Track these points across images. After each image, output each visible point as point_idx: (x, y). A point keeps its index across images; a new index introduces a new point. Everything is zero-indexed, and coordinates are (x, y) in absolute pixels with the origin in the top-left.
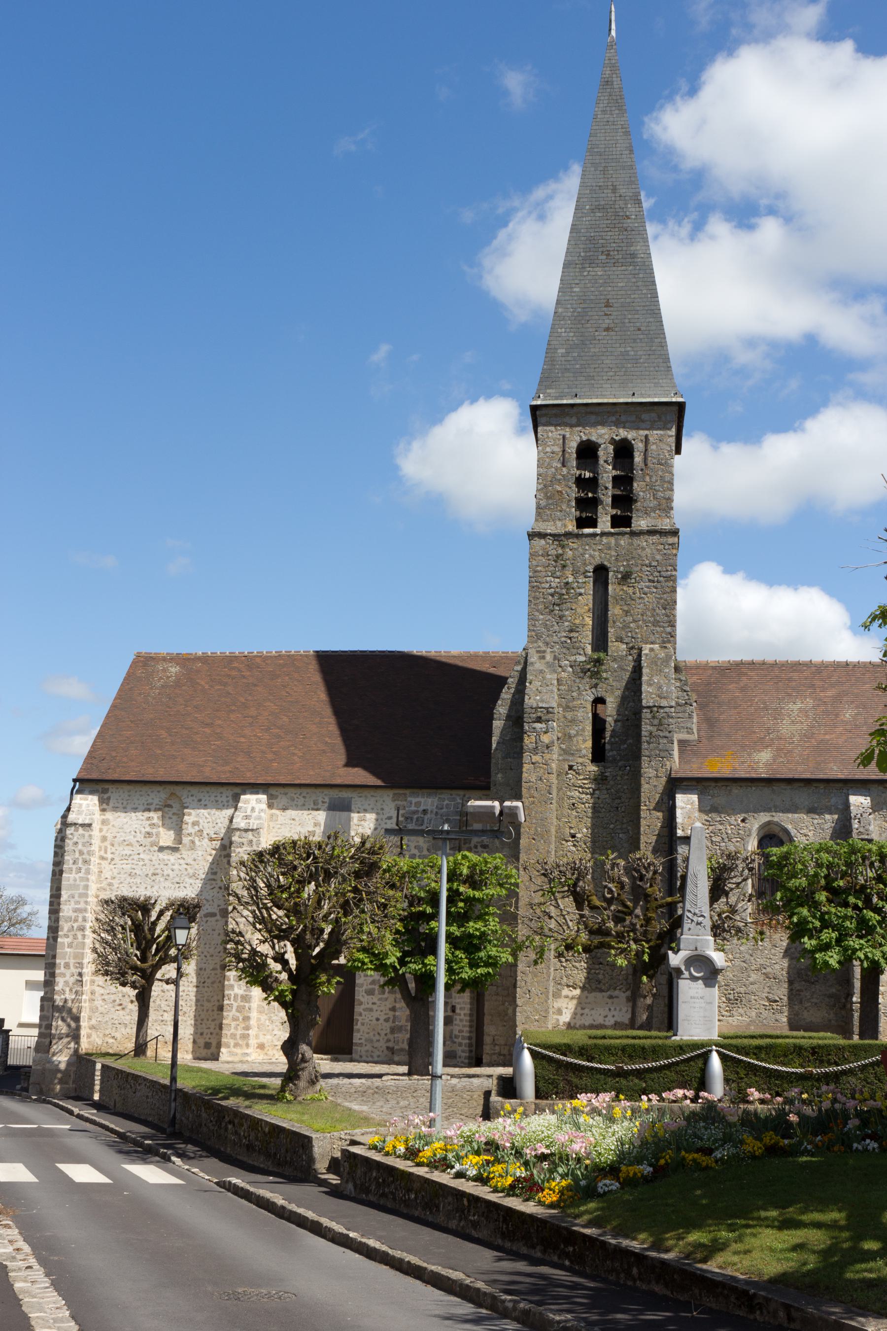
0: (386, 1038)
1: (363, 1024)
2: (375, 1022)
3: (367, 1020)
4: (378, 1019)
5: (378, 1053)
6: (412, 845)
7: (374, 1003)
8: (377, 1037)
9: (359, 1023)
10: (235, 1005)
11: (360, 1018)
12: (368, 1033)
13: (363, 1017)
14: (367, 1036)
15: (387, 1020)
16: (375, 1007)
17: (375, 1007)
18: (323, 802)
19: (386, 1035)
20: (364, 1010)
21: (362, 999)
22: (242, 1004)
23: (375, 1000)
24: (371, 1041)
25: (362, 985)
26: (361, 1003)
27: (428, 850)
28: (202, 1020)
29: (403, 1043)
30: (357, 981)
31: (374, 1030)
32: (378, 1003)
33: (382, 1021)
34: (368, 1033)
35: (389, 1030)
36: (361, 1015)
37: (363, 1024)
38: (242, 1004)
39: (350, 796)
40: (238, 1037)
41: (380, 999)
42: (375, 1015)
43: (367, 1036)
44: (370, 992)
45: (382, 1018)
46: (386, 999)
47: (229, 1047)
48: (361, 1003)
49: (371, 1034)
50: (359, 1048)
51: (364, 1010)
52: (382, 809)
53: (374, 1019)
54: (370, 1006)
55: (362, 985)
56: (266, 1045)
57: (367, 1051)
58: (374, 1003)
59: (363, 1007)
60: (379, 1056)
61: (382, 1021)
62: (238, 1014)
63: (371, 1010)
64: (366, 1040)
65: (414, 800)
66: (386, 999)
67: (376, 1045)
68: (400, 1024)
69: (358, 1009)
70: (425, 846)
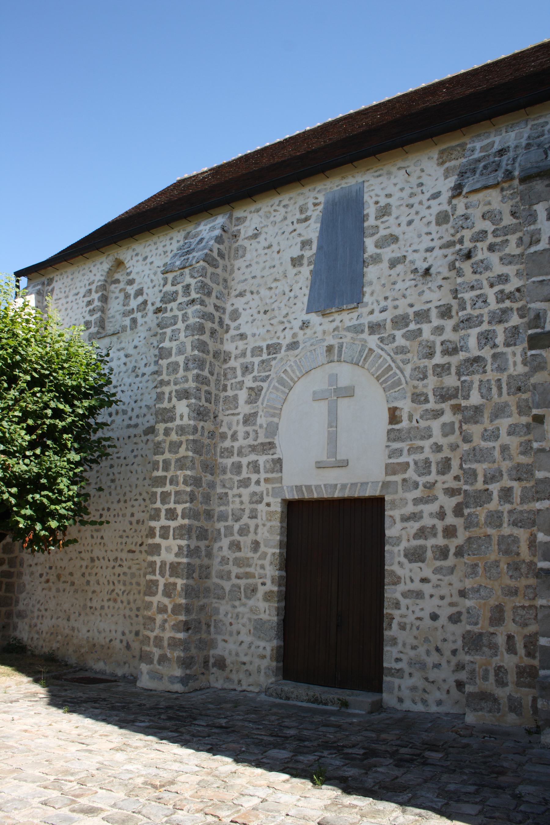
0: (454, 661)
1: (403, 627)
2: (428, 622)
3: (411, 618)
4: (434, 617)
5: (438, 695)
6: (476, 213)
7: (424, 580)
8: (435, 658)
9: (395, 625)
10: (162, 582)
11: (396, 613)
12: (414, 648)
13: (403, 610)
14: (412, 653)
15: (455, 619)
16: (427, 589)
17: (427, 589)
18: (315, 205)
19: (454, 652)
20: (405, 595)
21: (400, 572)
22: (172, 580)
23: (427, 573)
24: (423, 666)
25: (399, 539)
26: (397, 581)
27: (513, 214)
28: (138, 609)
29: (485, 678)
30: (388, 533)
31: (426, 640)
32: (434, 578)
33: (443, 620)
34: (414, 648)
35: (460, 643)
36: (397, 605)
37: (403, 627)
38: (172, 580)
39: (360, 180)
40: (166, 643)
41: (437, 571)
42: (430, 605)
43: (412, 653)
44: (416, 556)
45: (445, 613)
46: (452, 570)
47: (151, 662)
48: (397, 581)
49: (422, 650)
50: (397, 682)
51: (405, 595)
52: (421, 185)
53: (426, 615)
54: (417, 586)
55: (399, 539)
56: (228, 662)
57: (414, 689)
58: (424, 580)
59: (401, 588)
60: (439, 703)
61: (443, 620)
62: (166, 601)
63: (419, 595)
64: (410, 664)
65: (478, 145)
66: (452, 570)
67: (433, 675)
68: (476, 629)
69: (392, 593)
70: (506, 208)
